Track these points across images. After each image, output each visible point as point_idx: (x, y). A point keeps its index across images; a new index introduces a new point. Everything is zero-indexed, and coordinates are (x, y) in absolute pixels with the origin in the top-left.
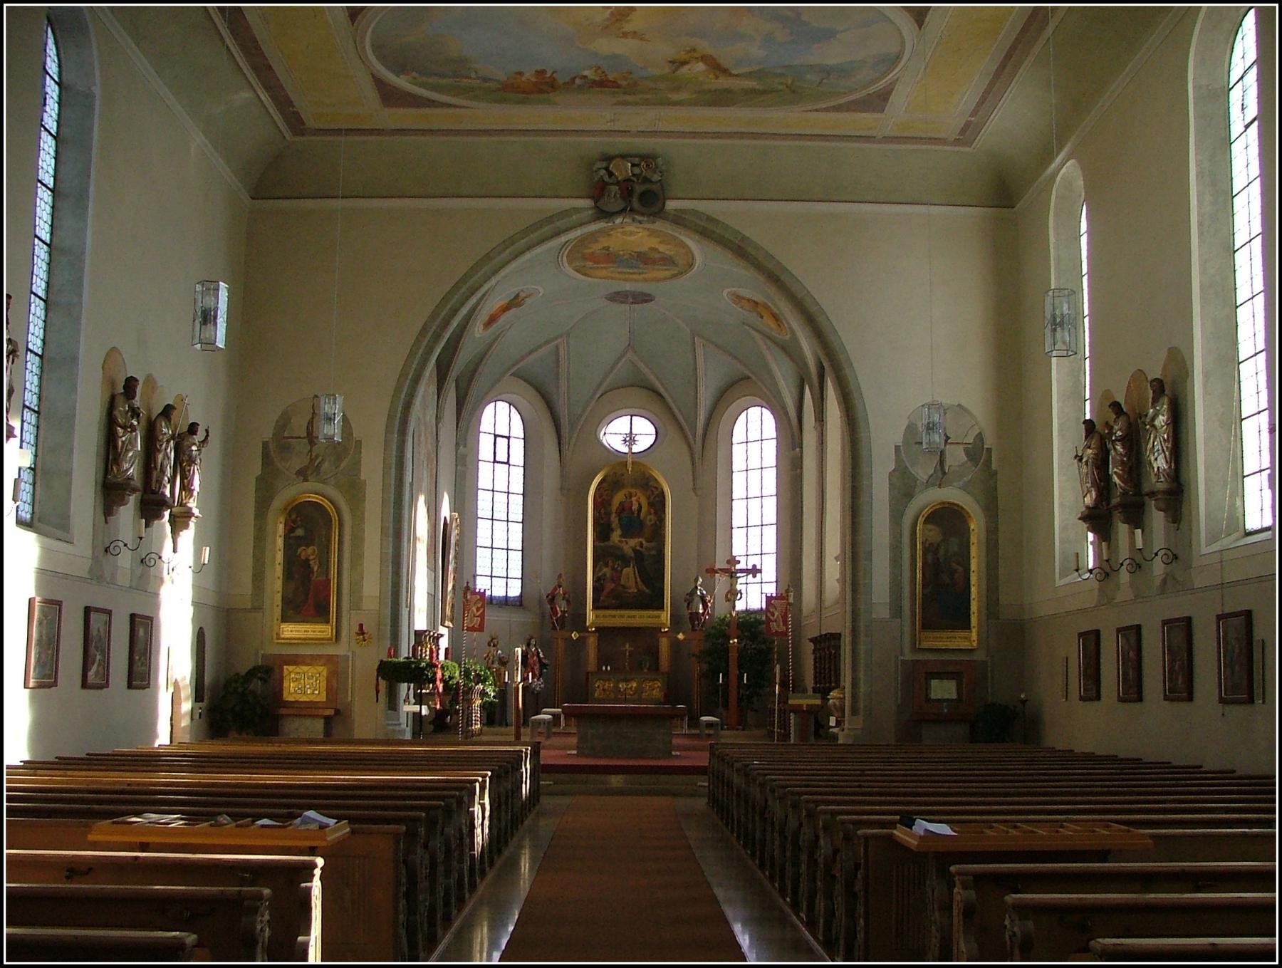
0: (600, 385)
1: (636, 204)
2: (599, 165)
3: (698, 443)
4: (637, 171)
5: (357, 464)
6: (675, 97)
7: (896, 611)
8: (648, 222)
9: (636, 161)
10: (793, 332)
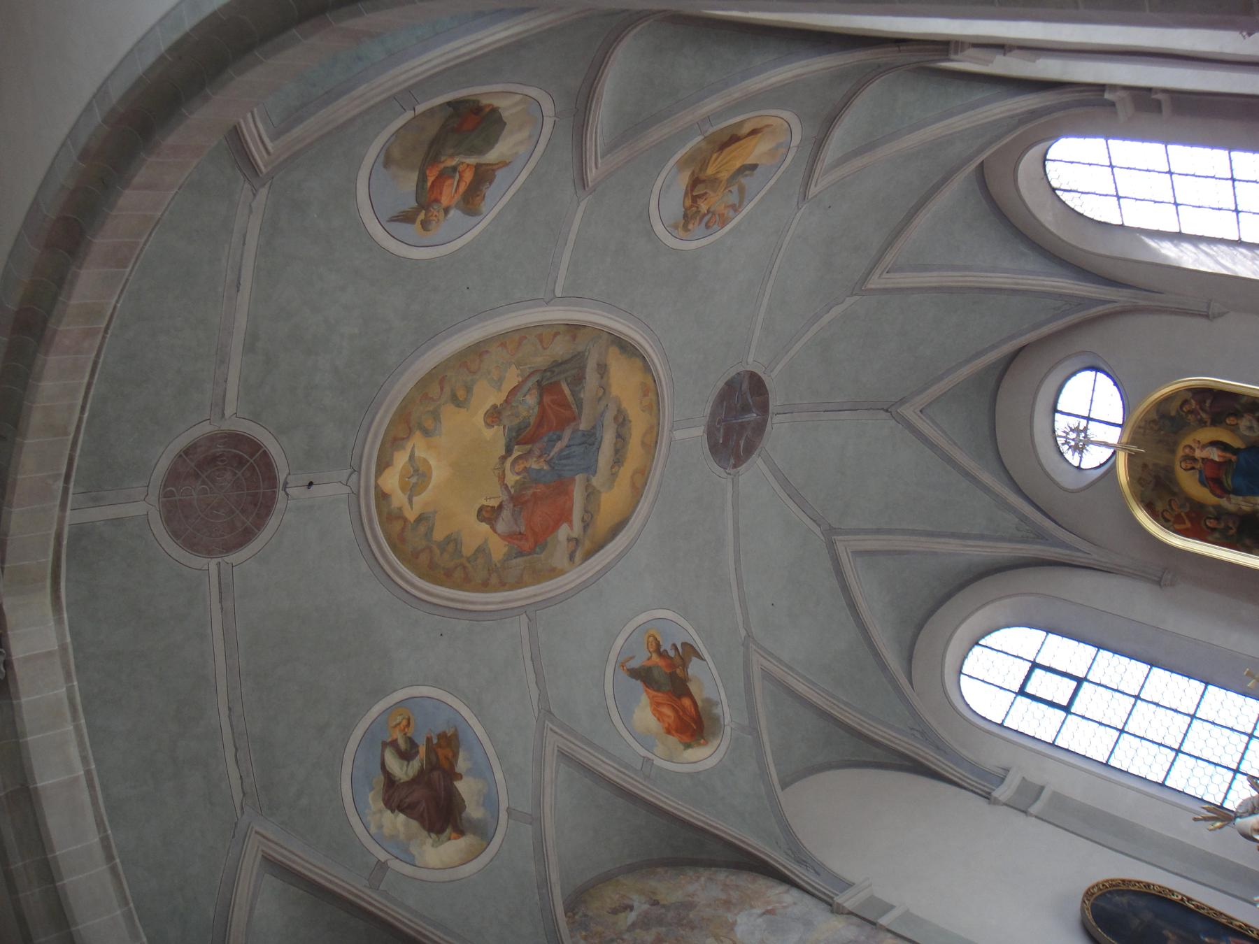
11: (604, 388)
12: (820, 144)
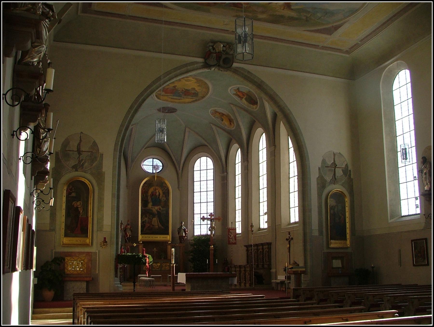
0: (144, 146)
1: (221, 63)
2: (211, 44)
3: (181, 170)
4: (224, 49)
5: (101, 164)
6: (261, 16)
7: (321, 232)
8: (224, 71)
9: (225, 44)
10: (238, 125)
11: (189, 98)
12: (224, 130)
